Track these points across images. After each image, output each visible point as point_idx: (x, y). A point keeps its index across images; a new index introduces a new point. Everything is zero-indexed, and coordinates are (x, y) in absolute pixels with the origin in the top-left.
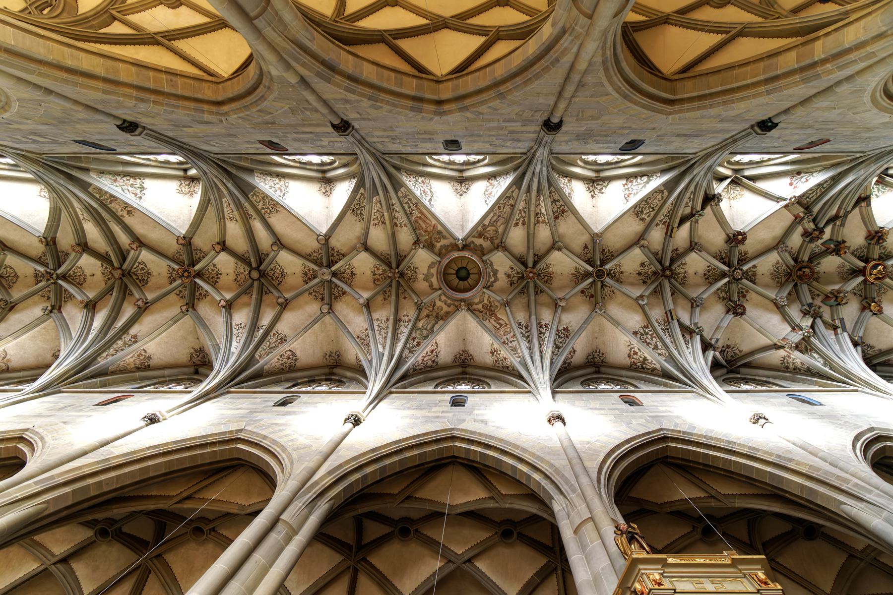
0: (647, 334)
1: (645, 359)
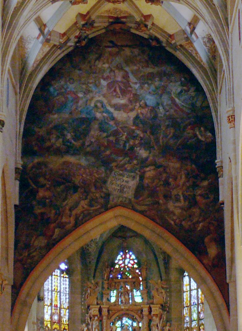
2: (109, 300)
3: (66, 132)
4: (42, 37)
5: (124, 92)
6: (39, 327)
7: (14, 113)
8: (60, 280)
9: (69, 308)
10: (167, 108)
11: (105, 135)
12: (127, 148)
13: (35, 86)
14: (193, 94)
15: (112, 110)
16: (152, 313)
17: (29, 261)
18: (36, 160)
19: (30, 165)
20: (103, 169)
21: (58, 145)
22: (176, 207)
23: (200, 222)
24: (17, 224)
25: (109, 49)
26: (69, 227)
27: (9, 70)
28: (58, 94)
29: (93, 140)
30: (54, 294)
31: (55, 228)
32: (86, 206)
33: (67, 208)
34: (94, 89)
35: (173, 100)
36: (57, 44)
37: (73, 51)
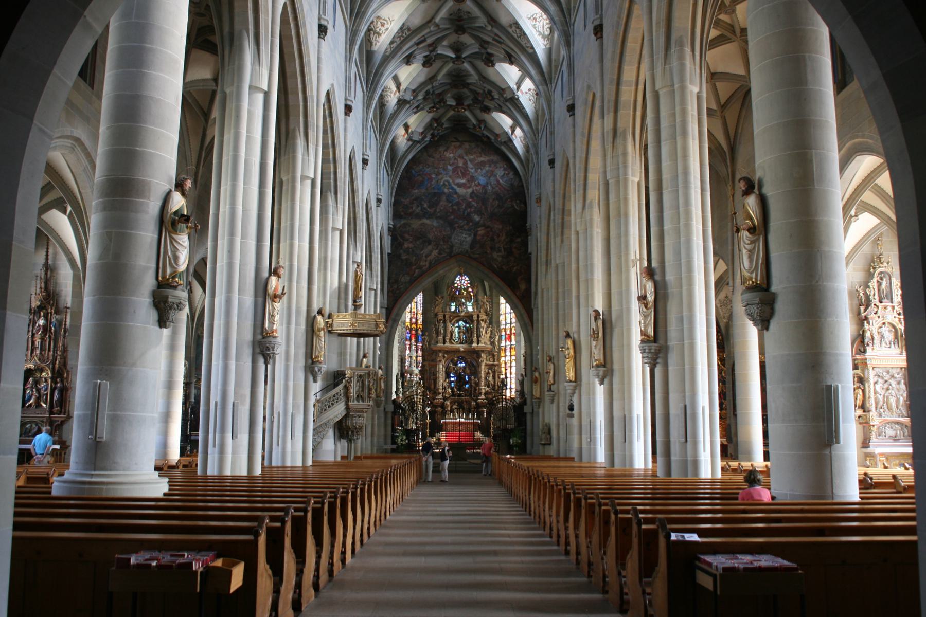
0: (403, 32)
1: (379, 34)
2: (450, 309)
3: (423, 203)
4: (406, 136)
5: (464, 174)
7: (387, 188)
9: (422, 314)
10: (494, 186)
11: (450, 204)
12: (466, 214)
13: (402, 170)
14: (512, 177)
15: (455, 187)
16: (480, 319)
17: (398, 291)
18: (403, 222)
19: (399, 225)
20: (448, 229)
21: (417, 211)
22: (498, 256)
23: (514, 267)
24: (389, 266)
25: (453, 144)
26: (424, 268)
27: (384, 163)
28: (418, 175)
29: (442, 208)
31: (415, 269)
32: (437, 254)
33: (424, 255)
34: (442, 172)
35: (498, 181)
36: (418, 140)
37: (427, 145)
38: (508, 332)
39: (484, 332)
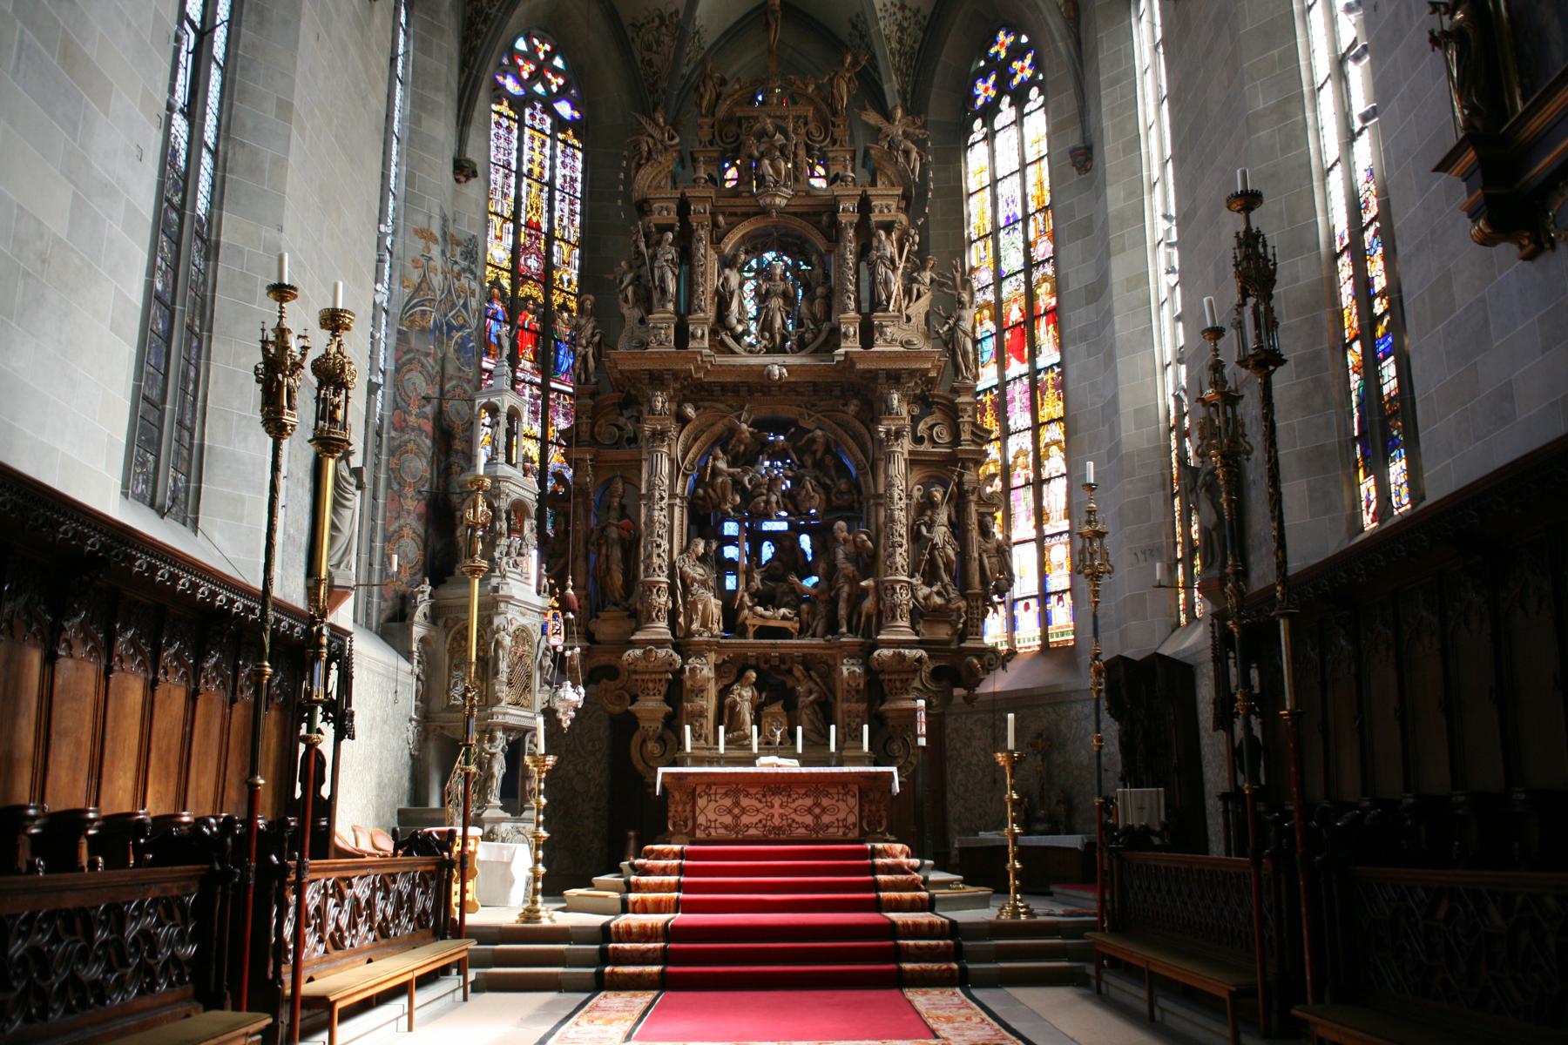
6: (456, 268)
8: (553, 148)
16: (875, 217)
30: (529, 185)
38: (1015, 314)
39: (896, 286)
